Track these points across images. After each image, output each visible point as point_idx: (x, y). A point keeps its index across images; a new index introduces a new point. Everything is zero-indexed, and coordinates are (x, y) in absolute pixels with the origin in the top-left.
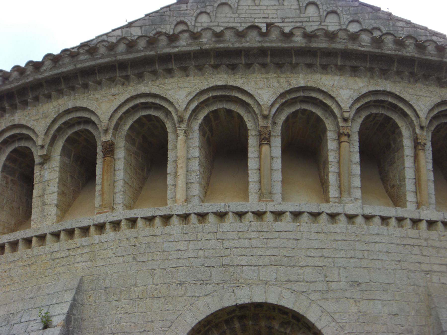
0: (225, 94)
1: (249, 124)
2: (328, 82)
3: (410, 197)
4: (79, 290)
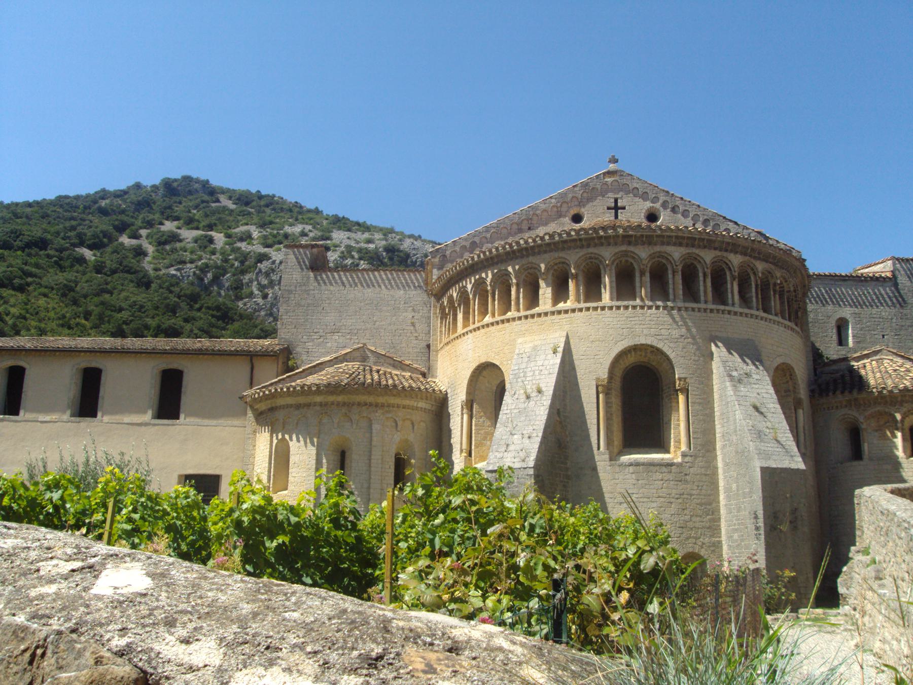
0: (625, 254)
1: (636, 267)
2: (670, 249)
3: (702, 298)
4: (567, 337)
